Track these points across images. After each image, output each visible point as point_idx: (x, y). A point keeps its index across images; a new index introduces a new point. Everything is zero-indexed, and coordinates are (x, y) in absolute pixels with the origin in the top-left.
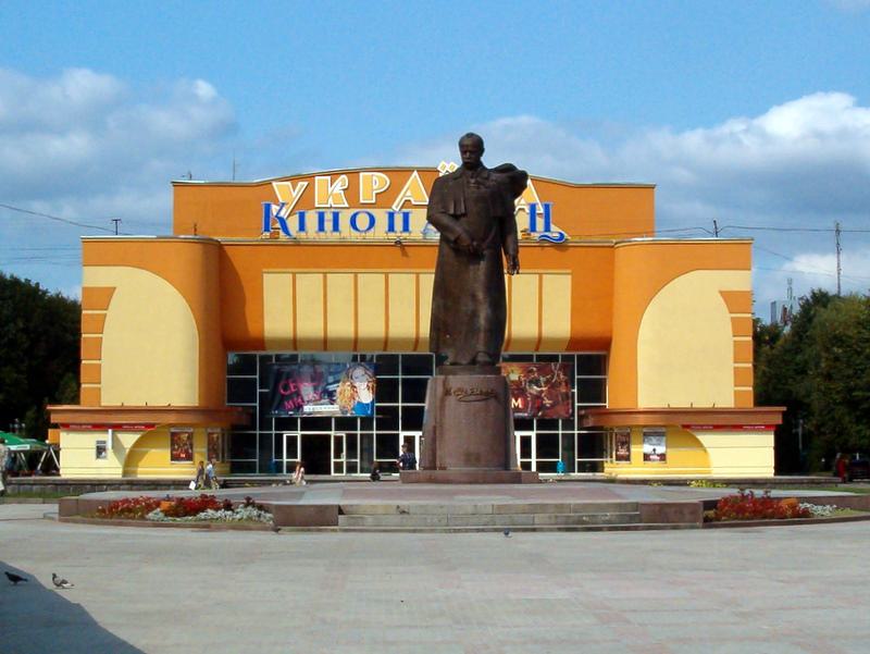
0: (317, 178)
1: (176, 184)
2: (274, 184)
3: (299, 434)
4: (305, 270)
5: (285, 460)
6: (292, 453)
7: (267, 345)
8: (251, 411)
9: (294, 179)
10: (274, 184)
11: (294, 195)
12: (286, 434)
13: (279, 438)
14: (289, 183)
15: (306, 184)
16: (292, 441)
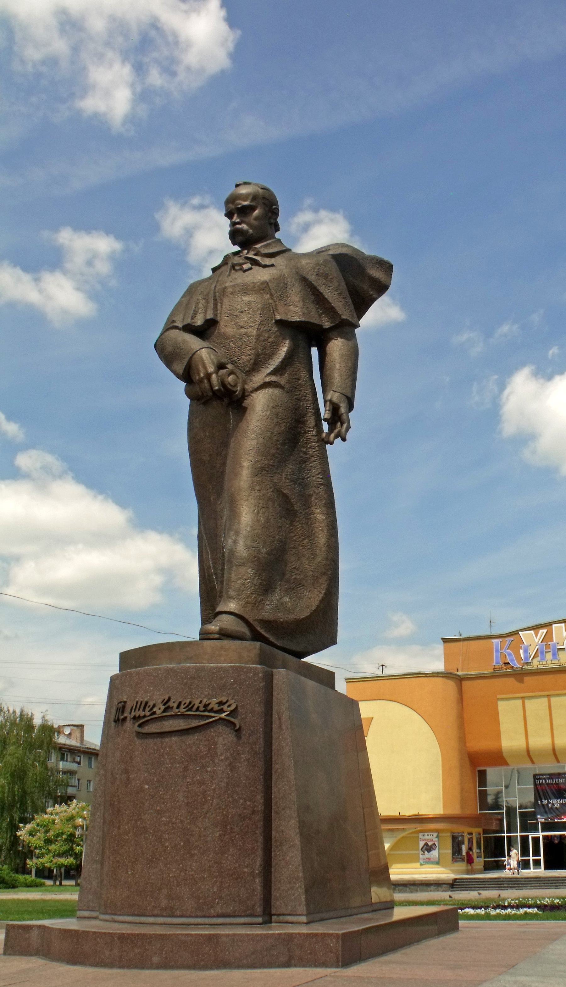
0: (553, 625)
1: (445, 641)
2: (520, 633)
3: (540, 835)
4: (533, 694)
5: (531, 858)
6: (536, 852)
7: (508, 760)
8: (499, 817)
9: (536, 628)
10: (520, 633)
11: (537, 640)
12: (531, 835)
13: (525, 840)
14: (532, 632)
15: (545, 631)
16: (536, 840)
